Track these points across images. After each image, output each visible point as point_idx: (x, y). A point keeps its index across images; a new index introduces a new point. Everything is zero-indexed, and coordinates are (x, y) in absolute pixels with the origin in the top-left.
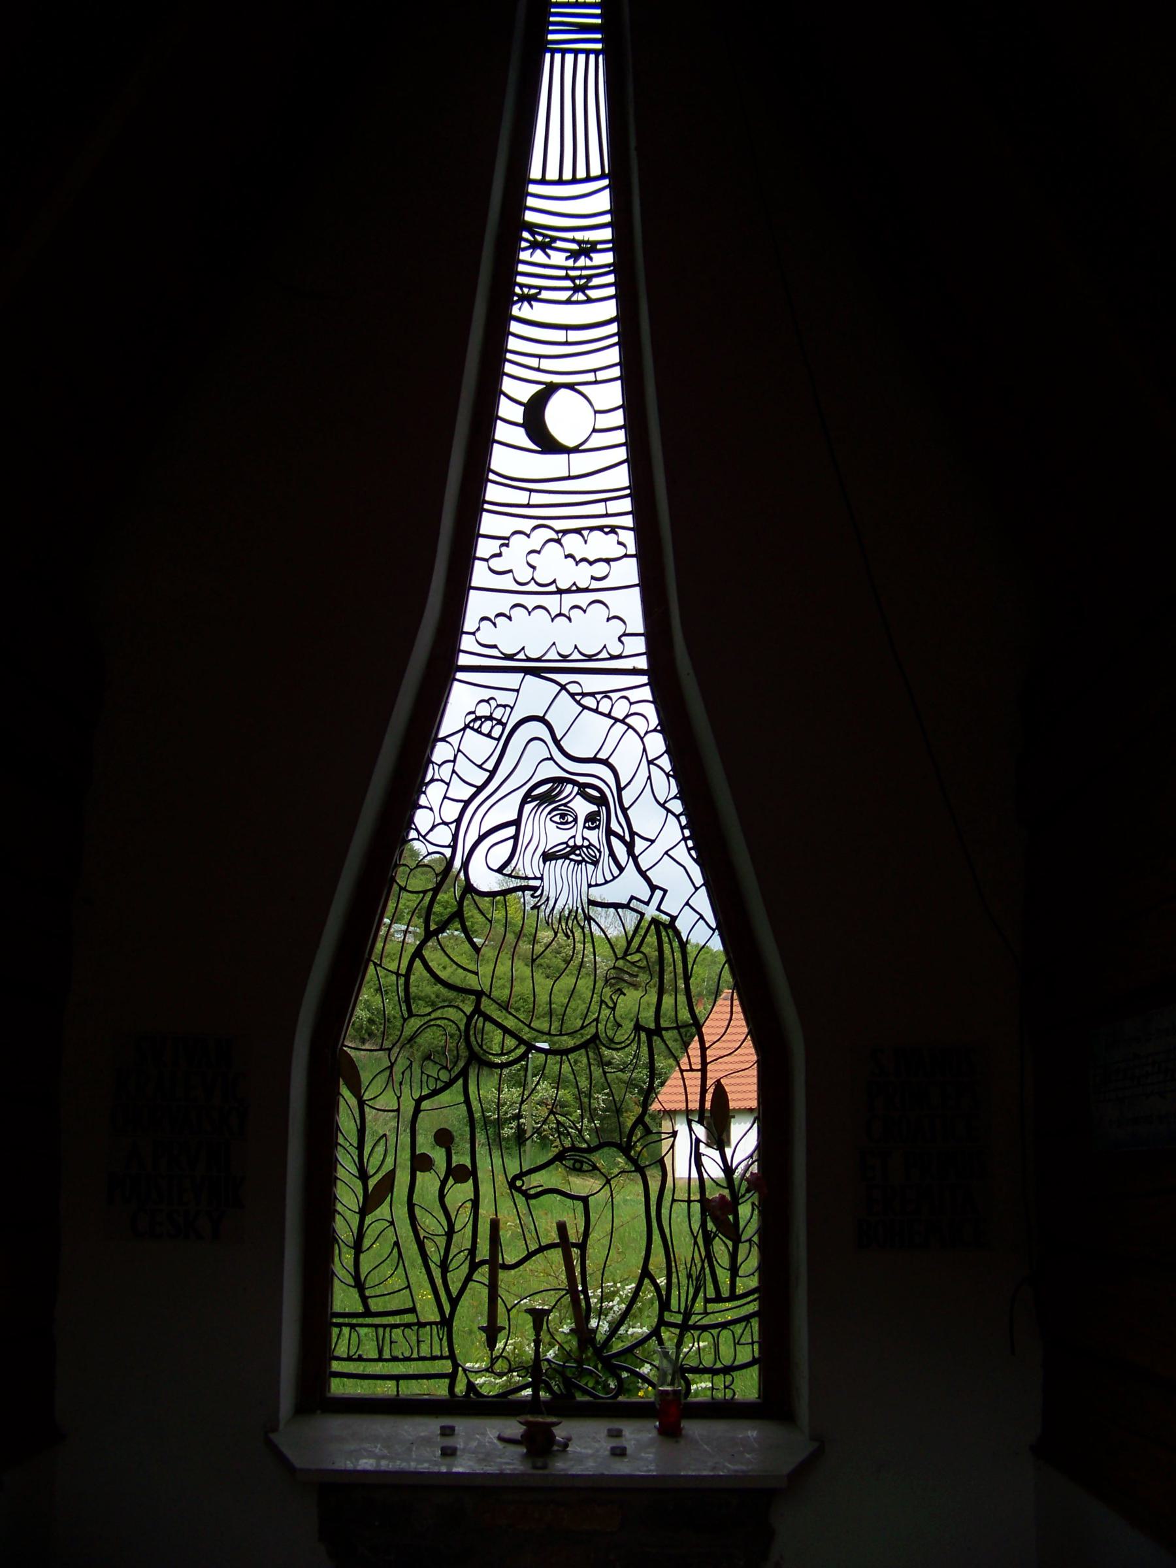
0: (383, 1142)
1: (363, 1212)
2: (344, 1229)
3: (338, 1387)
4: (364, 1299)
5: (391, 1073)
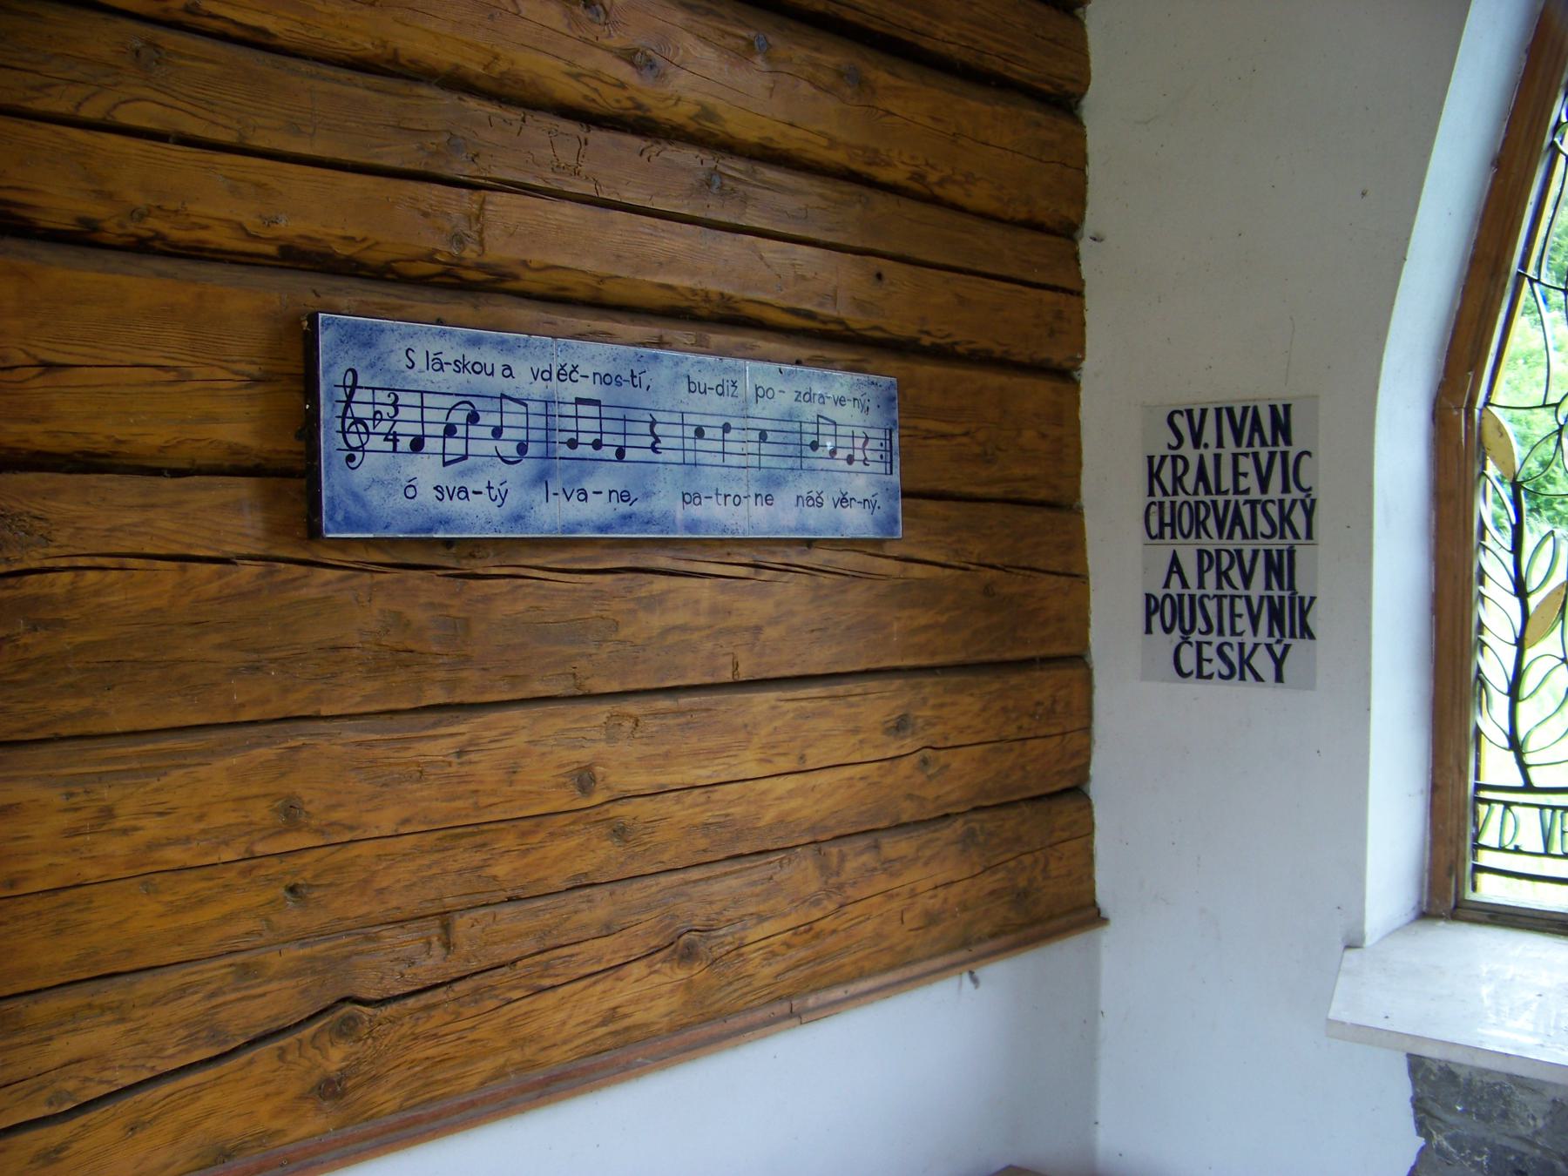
0: (1549, 543)
1: (1520, 643)
2: (1494, 664)
3: (1490, 890)
4: (1524, 768)
5: (1559, 443)
